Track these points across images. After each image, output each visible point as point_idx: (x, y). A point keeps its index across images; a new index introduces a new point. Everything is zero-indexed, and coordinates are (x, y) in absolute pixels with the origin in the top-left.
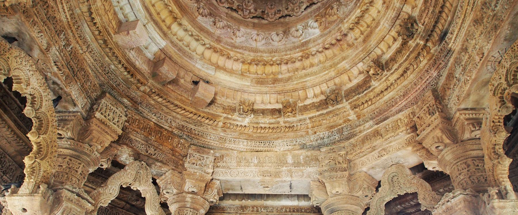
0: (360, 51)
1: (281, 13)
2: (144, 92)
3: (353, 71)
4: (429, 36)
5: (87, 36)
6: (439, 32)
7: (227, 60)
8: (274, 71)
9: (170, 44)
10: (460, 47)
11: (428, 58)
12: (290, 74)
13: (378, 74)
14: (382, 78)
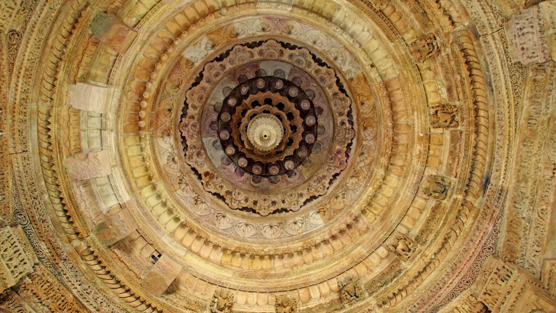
0: (379, 231)
1: (277, 205)
2: (77, 250)
3: (372, 260)
4: (468, 185)
5: (30, 144)
6: (479, 181)
7: (204, 247)
8: (264, 267)
9: (135, 203)
10: (514, 181)
11: (473, 215)
12: (287, 270)
13: (410, 250)
14: (415, 257)
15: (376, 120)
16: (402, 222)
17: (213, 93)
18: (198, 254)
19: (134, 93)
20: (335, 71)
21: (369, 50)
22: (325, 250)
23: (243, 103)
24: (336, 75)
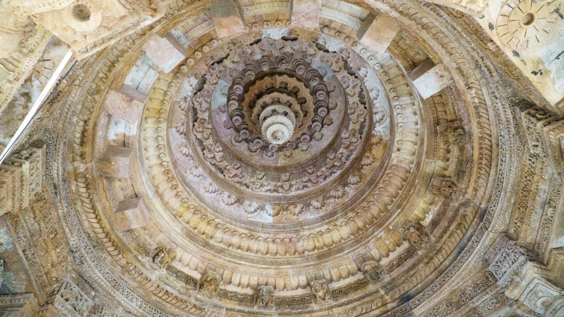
23: (274, 77)
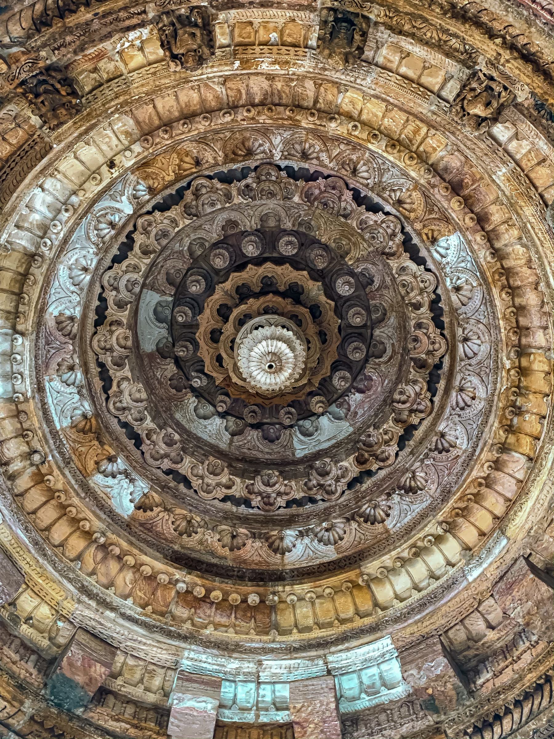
13: (489, 88)
15: (228, 134)
16: (436, 89)
17: (209, 440)
18: (512, 504)
19: (198, 611)
20: (141, 216)
21: (82, 174)
22: (508, 238)
24: (149, 213)
